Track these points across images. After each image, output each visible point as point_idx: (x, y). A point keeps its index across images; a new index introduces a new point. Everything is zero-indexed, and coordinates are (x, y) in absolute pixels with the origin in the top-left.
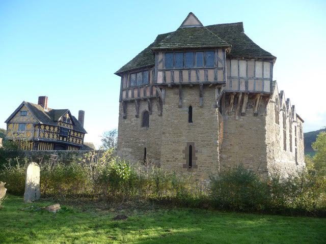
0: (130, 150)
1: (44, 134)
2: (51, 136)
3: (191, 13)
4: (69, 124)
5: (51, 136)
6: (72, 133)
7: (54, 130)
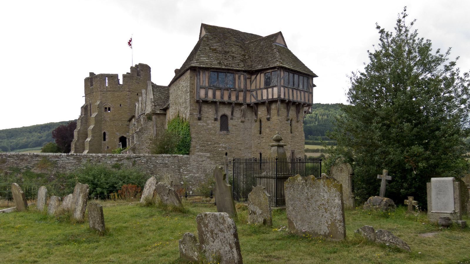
0: (208, 155)
3: (280, 33)
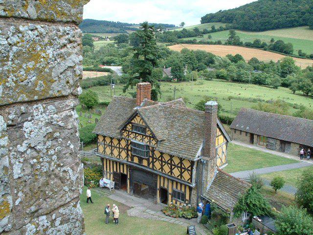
1: (105, 149)
2: (116, 152)
4: (147, 136)
5: (116, 152)
6: (157, 155)
7: (119, 143)
